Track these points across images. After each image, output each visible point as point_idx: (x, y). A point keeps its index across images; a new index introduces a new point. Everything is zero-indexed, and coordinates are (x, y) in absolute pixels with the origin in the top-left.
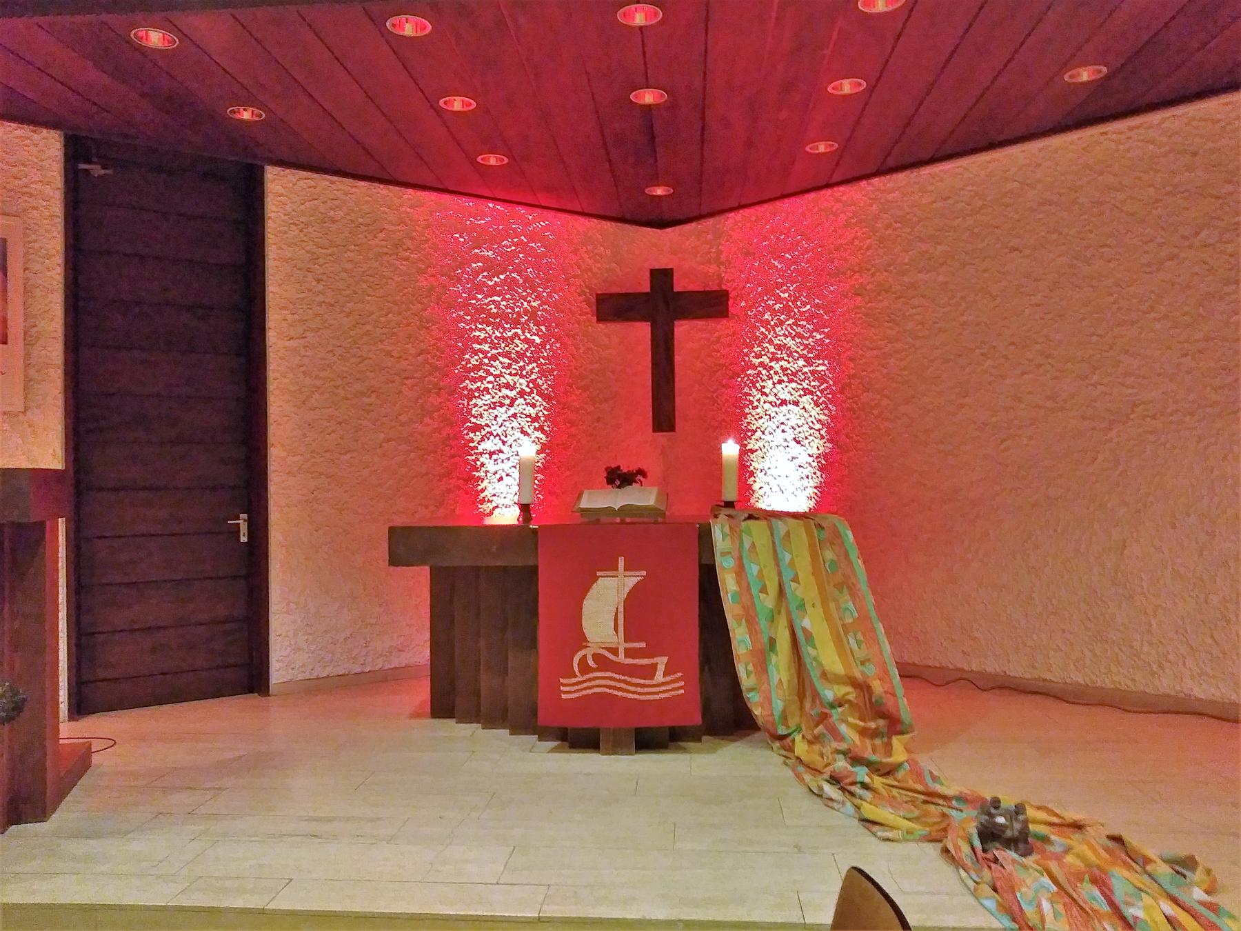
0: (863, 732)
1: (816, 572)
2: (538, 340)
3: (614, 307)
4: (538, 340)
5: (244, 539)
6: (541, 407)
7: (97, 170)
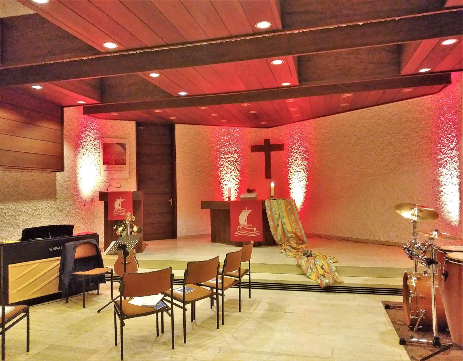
0: (297, 243)
1: (286, 210)
2: (237, 157)
3: (255, 148)
4: (237, 157)
5: (172, 205)
6: (238, 174)
7: (142, 128)
